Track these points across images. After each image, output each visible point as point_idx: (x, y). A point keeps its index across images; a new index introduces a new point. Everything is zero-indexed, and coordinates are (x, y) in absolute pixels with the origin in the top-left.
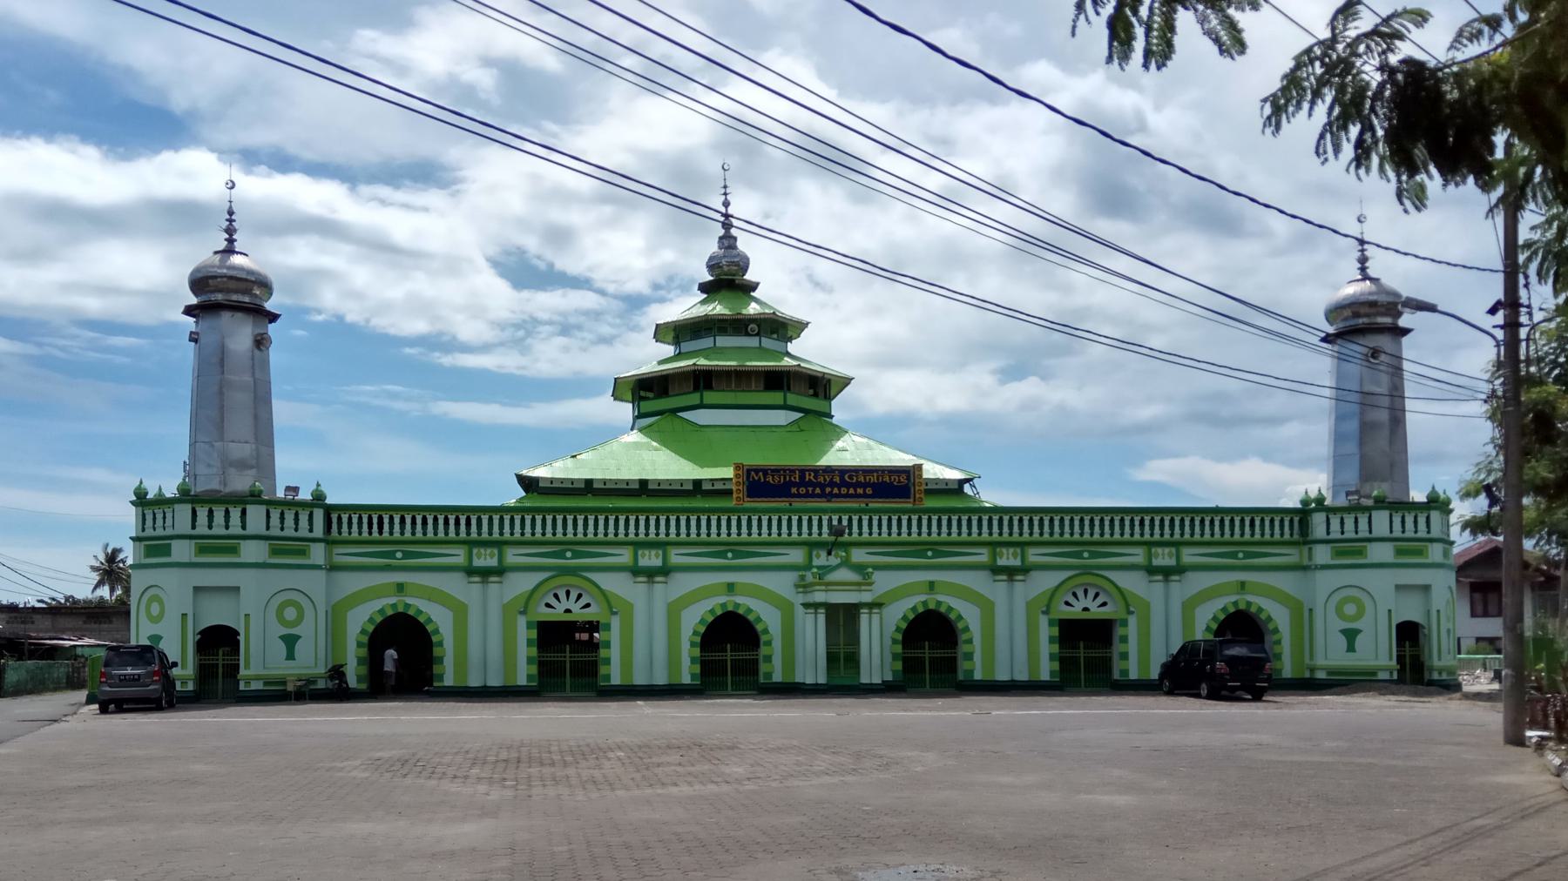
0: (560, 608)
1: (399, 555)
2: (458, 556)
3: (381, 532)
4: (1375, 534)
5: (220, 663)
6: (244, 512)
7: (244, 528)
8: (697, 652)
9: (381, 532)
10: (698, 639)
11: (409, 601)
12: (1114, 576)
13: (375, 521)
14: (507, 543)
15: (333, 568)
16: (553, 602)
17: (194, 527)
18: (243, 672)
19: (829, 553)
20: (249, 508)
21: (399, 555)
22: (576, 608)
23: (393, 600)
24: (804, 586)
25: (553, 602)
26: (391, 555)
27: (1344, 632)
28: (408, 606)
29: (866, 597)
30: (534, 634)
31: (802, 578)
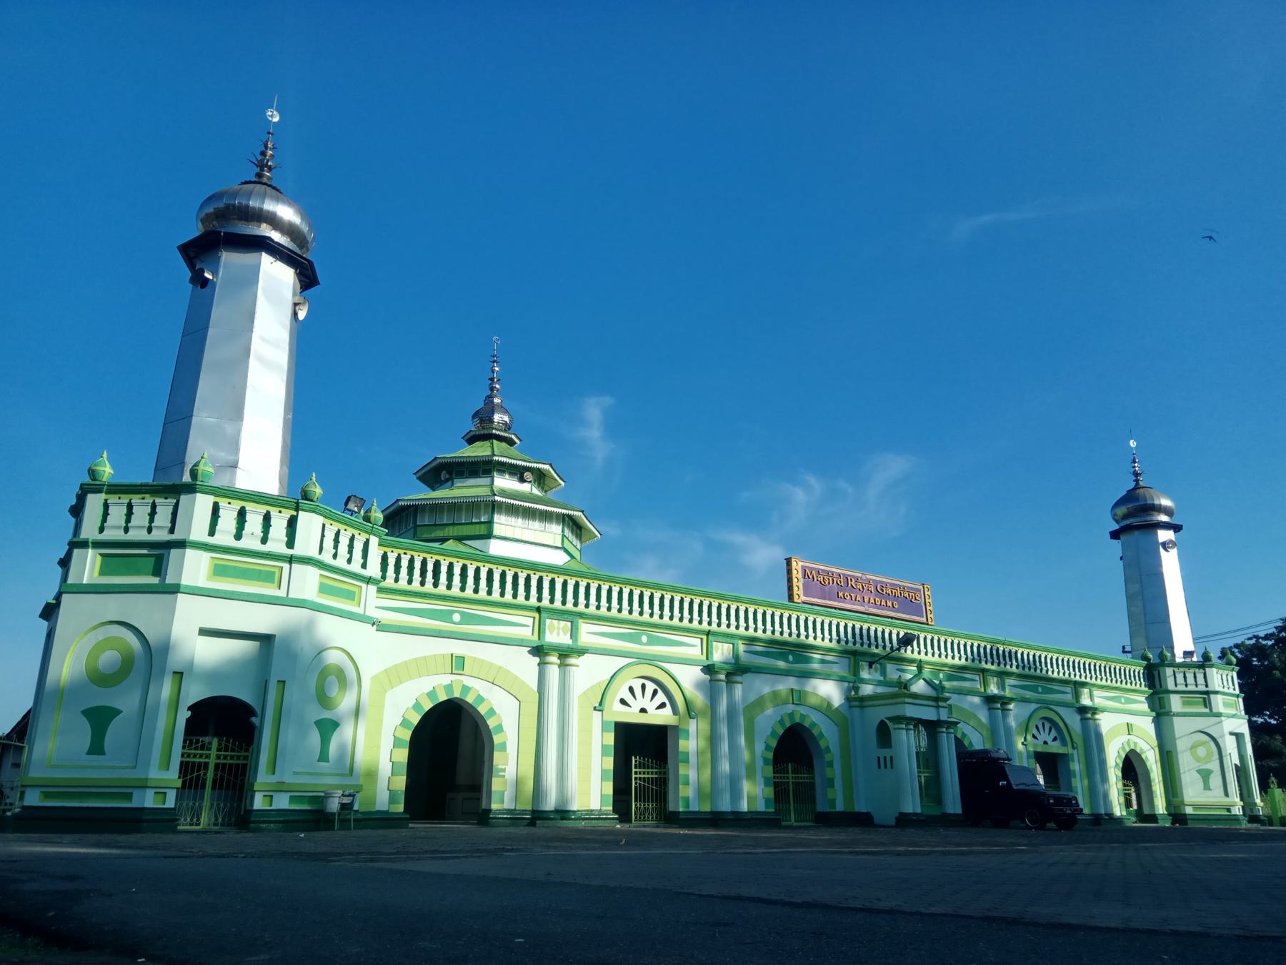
0: (636, 705)
1: (456, 617)
2: (523, 626)
3: (436, 585)
4: (1210, 689)
5: (212, 761)
6: (292, 523)
7: (290, 543)
8: (769, 771)
9: (436, 585)
10: (770, 755)
11: (469, 682)
12: (1060, 710)
13: (430, 567)
14: (581, 615)
15: (381, 627)
16: (629, 698)
17: (212, 532)
18: (263, 778)
19: (870, 667)
20: (302, 516)
21: (456, 617)
22: (651, 707)
23: (446, 679)
24: (862, 699)
25: (629, 698)
26: (446, 616)
27: (1199, 771)
28: (466, 689)
29: (944, 716)
30: (610, 739)
31: (857, 689)
